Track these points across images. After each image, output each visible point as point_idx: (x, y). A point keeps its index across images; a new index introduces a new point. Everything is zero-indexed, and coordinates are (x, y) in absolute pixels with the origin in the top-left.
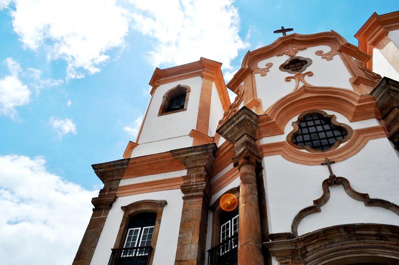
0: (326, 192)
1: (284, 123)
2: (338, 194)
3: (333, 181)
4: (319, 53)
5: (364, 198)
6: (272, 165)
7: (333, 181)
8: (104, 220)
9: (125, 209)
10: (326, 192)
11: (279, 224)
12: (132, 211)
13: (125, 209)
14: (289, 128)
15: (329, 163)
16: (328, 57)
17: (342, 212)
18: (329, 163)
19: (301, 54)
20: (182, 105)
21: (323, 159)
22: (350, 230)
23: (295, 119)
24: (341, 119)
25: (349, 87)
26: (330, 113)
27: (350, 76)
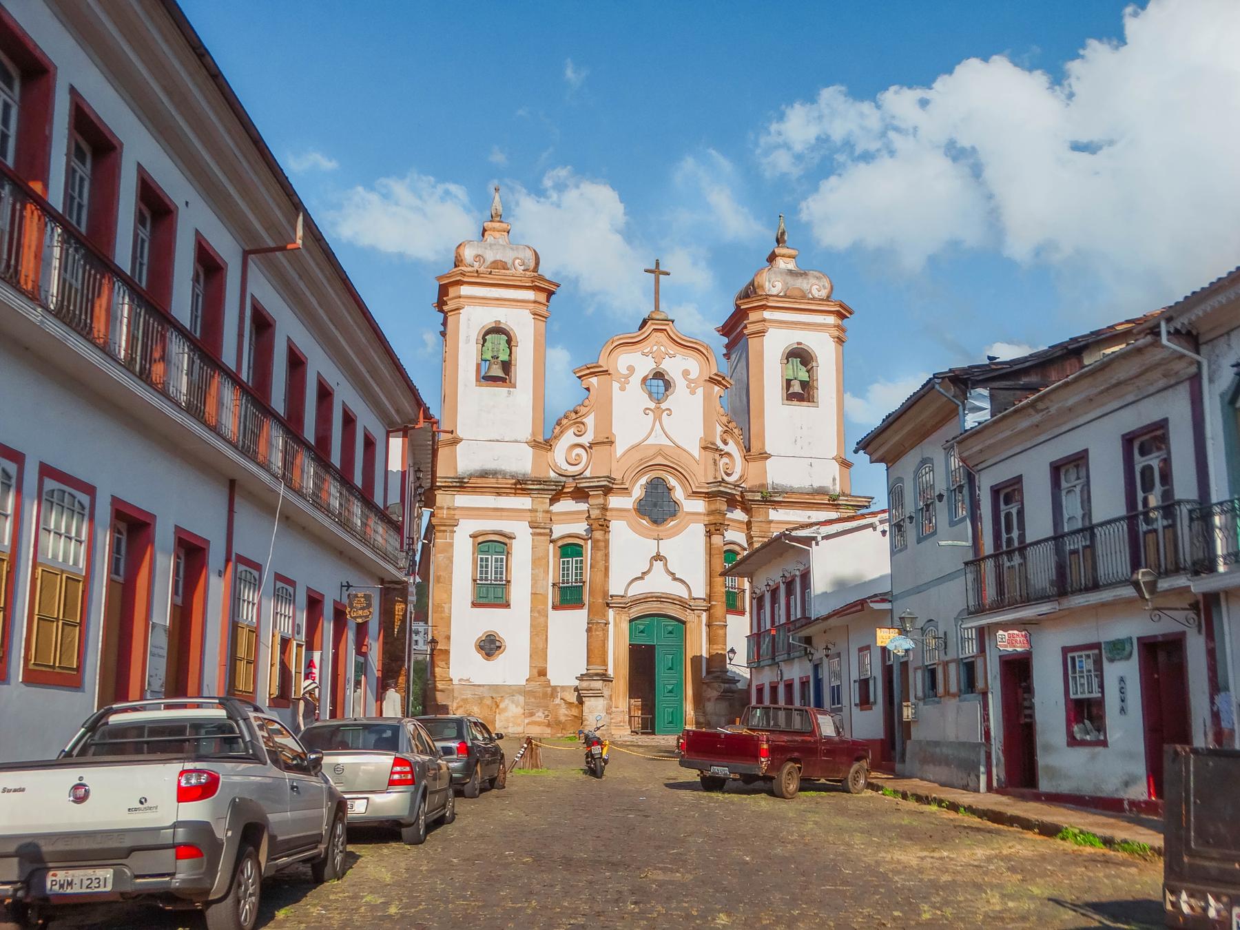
0: (651, 565)
1: (634, 480)
2: (658, 565)
3: (658, 557)
4: (686, 373)
5: (673, 574)
6: (618, 528)
7: (658, 557)
8: (451, 545)
9: (473, 536)
10: (651, 565)
11: (616, 587)
12: (480, 539)
13: (473, 536)
14: (638, 492)
15: (659, 539)
16: (692, 387)
17: (658, 583)
18: (659, 539)
19: (668, 366)
20: (504, 357)
21: (655, 535)
22: (659, 598)
23: (643, 480)
24: (679, 494)
25: (696, 452)
26: (672, 482)
27: (700, 433)
